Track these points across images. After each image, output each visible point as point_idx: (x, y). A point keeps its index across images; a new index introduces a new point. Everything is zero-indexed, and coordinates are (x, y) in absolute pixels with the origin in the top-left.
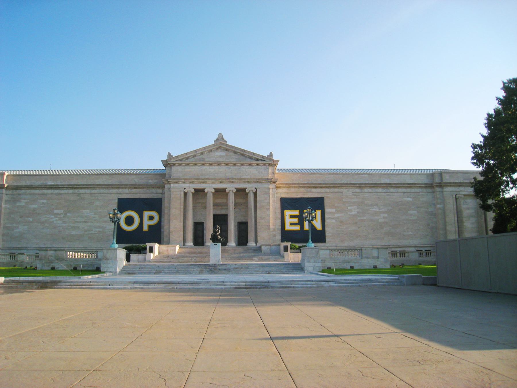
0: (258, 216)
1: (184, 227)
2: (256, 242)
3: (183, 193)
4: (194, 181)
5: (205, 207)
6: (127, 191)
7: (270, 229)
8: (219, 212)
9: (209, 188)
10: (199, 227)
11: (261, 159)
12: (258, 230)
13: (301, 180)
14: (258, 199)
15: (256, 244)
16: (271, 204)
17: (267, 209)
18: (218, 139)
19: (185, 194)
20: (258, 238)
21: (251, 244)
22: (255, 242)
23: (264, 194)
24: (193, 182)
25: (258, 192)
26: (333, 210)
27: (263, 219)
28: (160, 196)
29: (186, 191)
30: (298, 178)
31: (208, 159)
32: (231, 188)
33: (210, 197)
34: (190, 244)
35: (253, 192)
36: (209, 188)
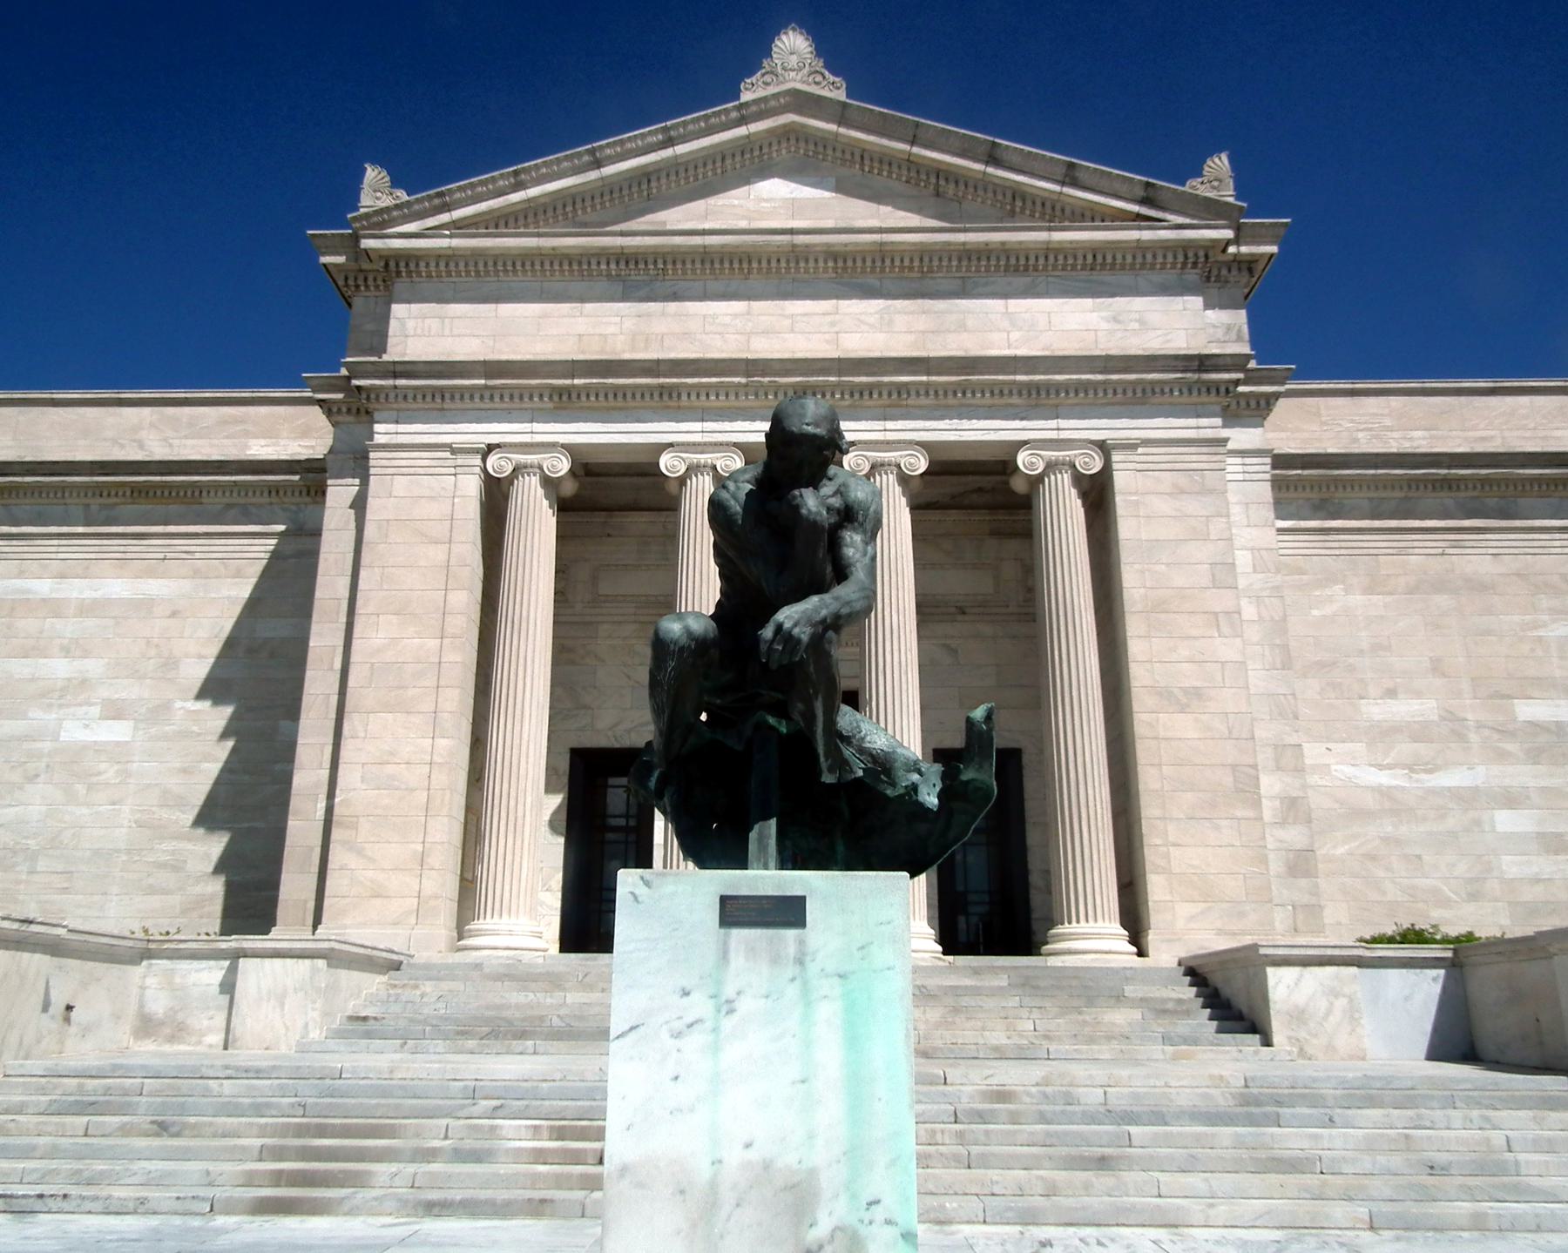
0: (1140, 675)
2: (1134, 921)
3: (471, 486)
4: (568, 391)
7: (1257, 803)
11: (1135, 208)
12: (1149, 810)
13: (1419, 434)
14: (1128, 528)
15: (1141, 953)
16: (1242, 583)
17: (1216, 614)
20: (1157, 889)
22: (1124, 925)
23: (1179, 492)
24: (565, 403)
25: (1121, 480)
27: (1183, 709)
29: (499, 464)
30: (1388, 422)
35: (1079, 479)
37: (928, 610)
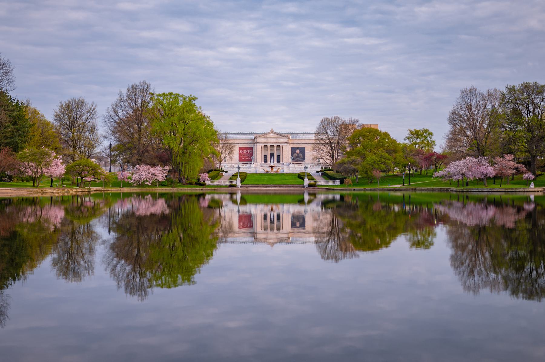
1: (261, 156)
5: (267, 151)
6: (241, 145)
8: (271, 152)
9: (269, 145)
10: (265, 157)
18: (271, 130)
19: (261, 147)
21: (281, 162)
26: (308, 152)
28: (252, 147)
31: (268, 136)
32: (275, 145)
33: (269, 148)
34: (263, 162)
36: (269, 145)
37: (277, 150)
